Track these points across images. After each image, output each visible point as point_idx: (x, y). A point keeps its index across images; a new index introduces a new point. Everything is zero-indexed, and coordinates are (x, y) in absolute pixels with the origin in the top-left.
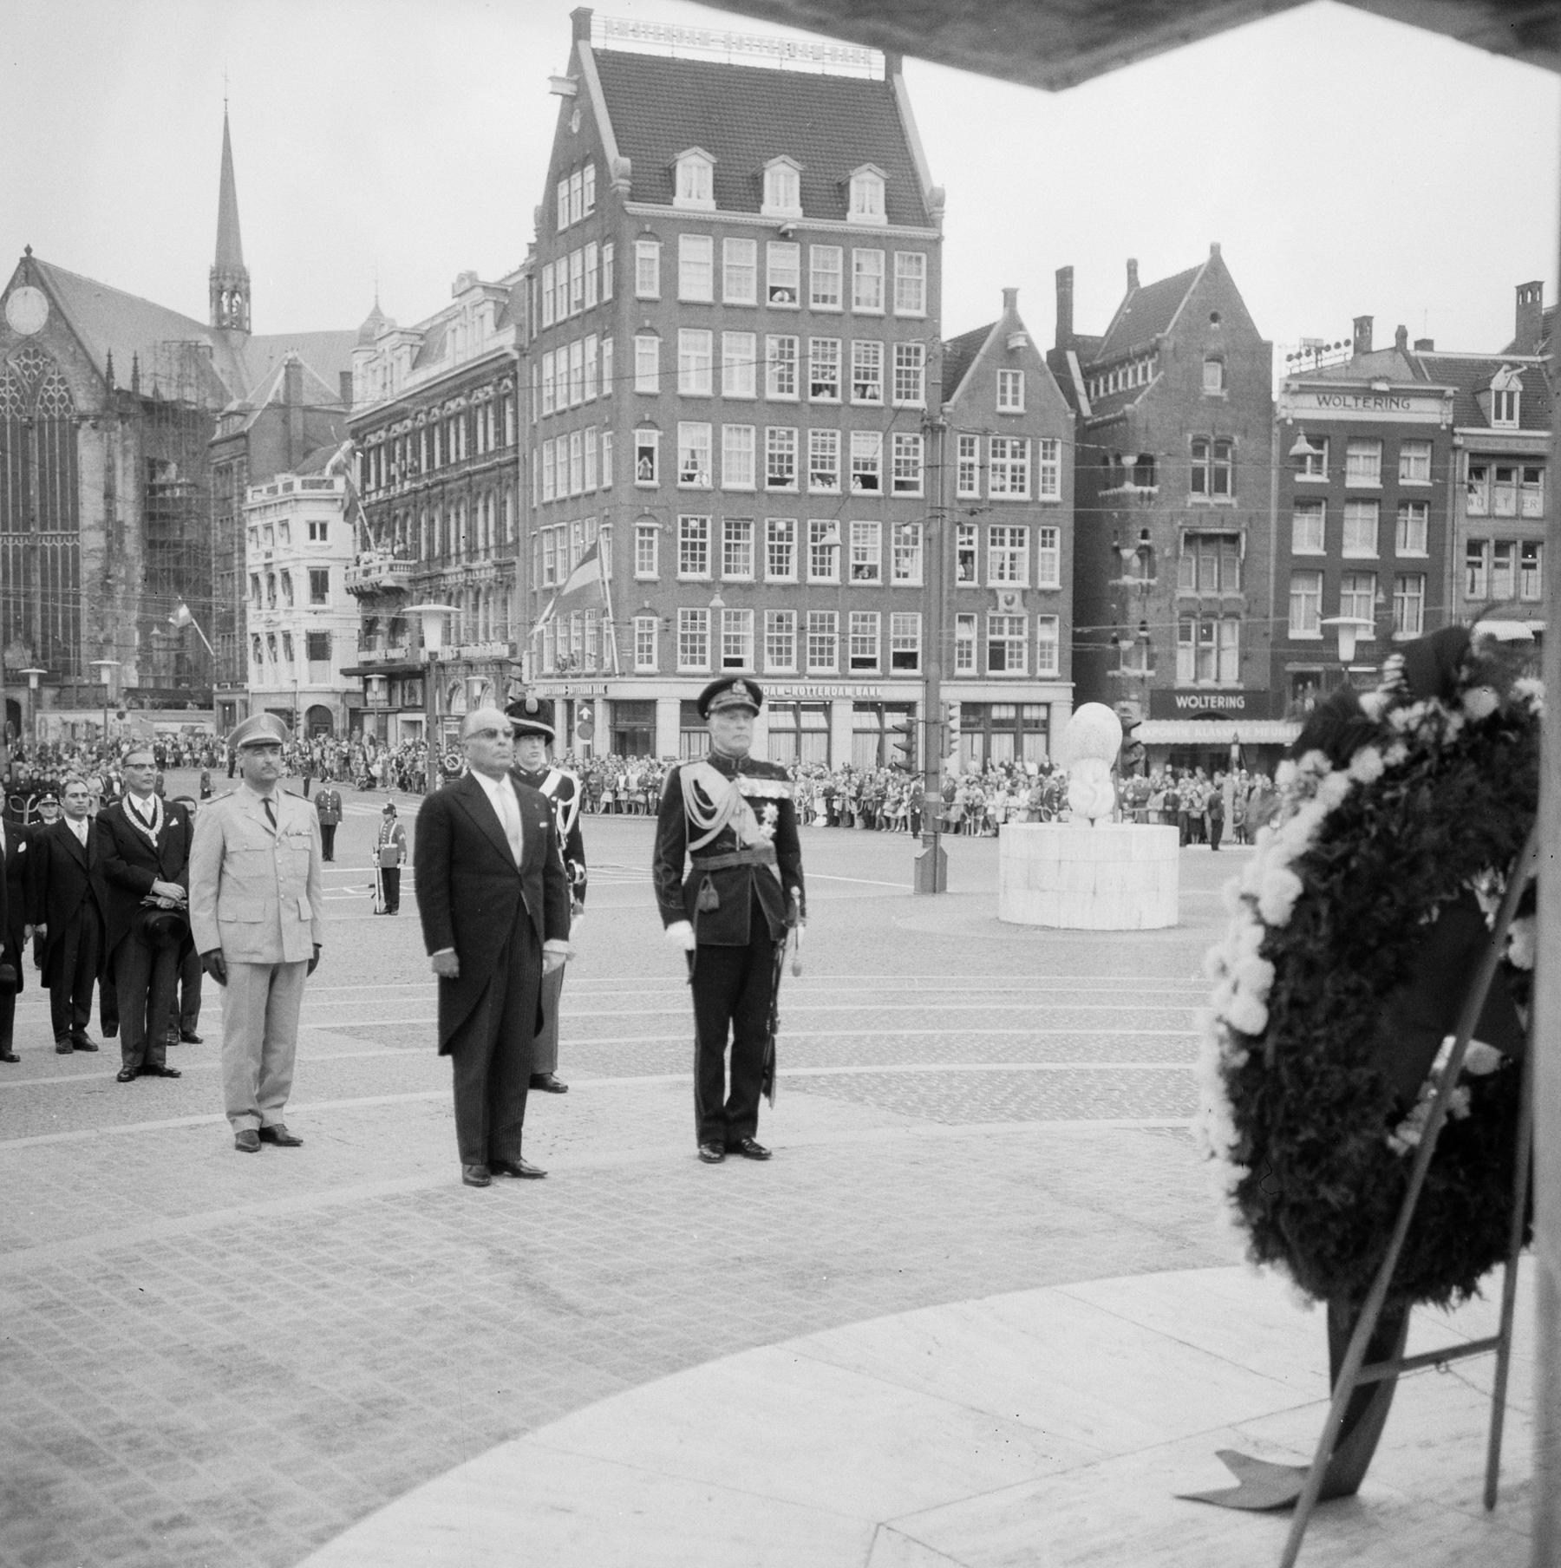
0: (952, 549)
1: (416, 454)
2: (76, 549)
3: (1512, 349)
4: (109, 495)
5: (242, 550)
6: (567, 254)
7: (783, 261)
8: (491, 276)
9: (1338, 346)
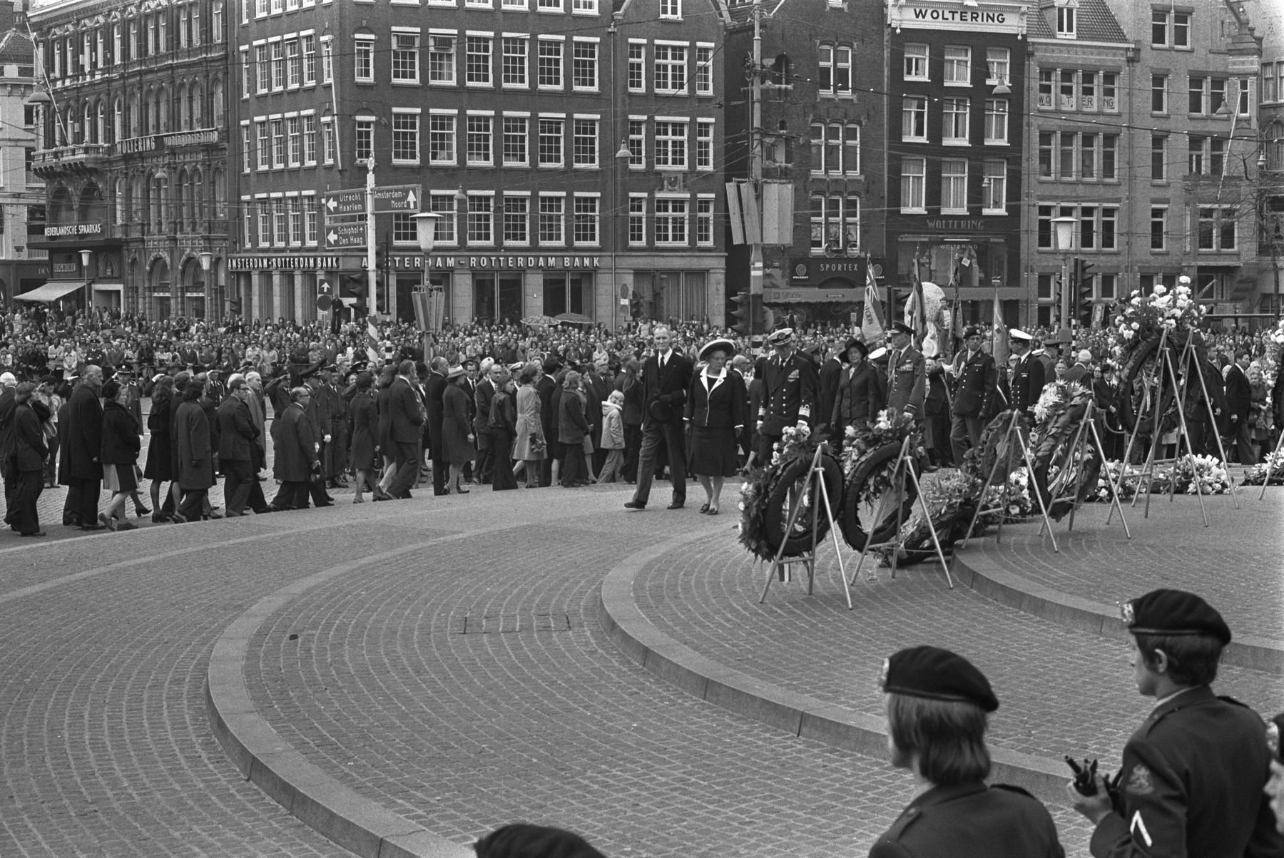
1: (109, 47)
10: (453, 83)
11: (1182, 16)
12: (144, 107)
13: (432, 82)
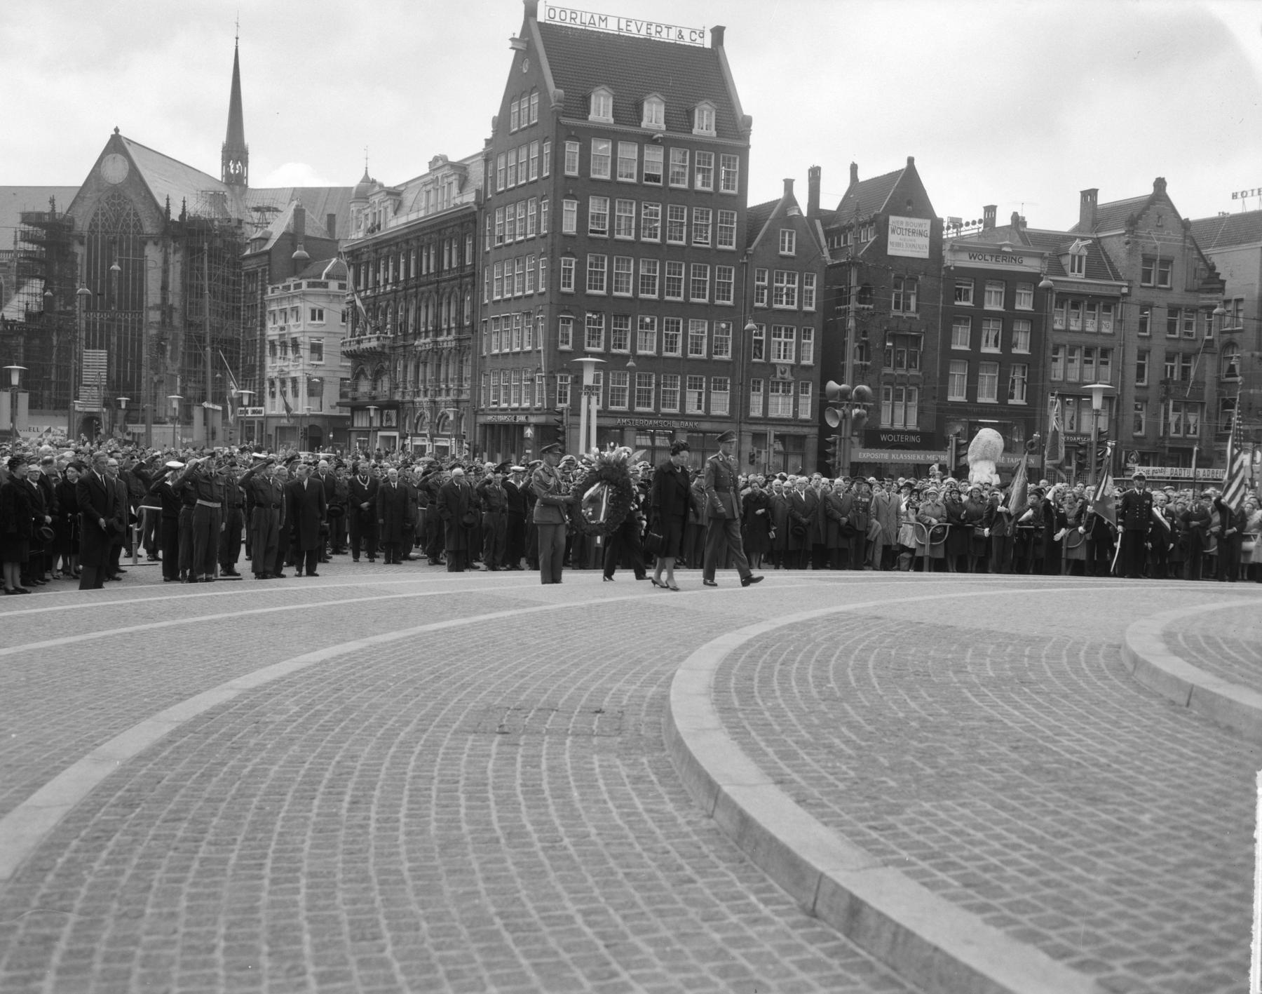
1: (396, 269)
2: (140, 321)
3: (1078, 228)
4: (164, 288)
5: (263, 325)
6: (517, 148)
7: (654, 157)
8: (454, 157)
9: (974, 223)
10: (630, 294)
11: (1166, 262)
12: (418, 309)
13: (616, 294)
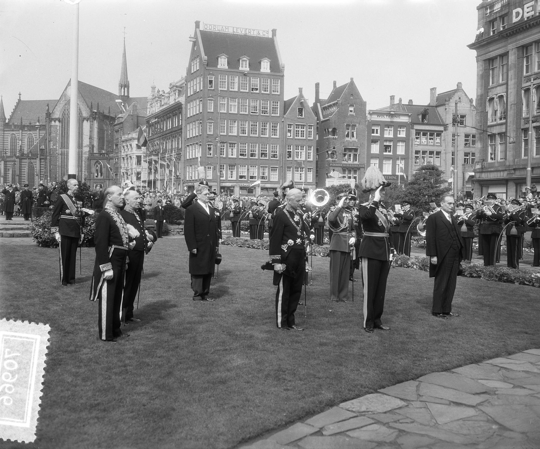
0: (286, 151)
2: (82, 152)
4: (91, 138)
10: (236, 134)
12: (166, 143)
13: (230, 134)
